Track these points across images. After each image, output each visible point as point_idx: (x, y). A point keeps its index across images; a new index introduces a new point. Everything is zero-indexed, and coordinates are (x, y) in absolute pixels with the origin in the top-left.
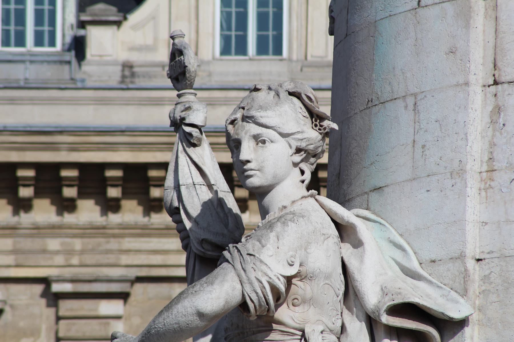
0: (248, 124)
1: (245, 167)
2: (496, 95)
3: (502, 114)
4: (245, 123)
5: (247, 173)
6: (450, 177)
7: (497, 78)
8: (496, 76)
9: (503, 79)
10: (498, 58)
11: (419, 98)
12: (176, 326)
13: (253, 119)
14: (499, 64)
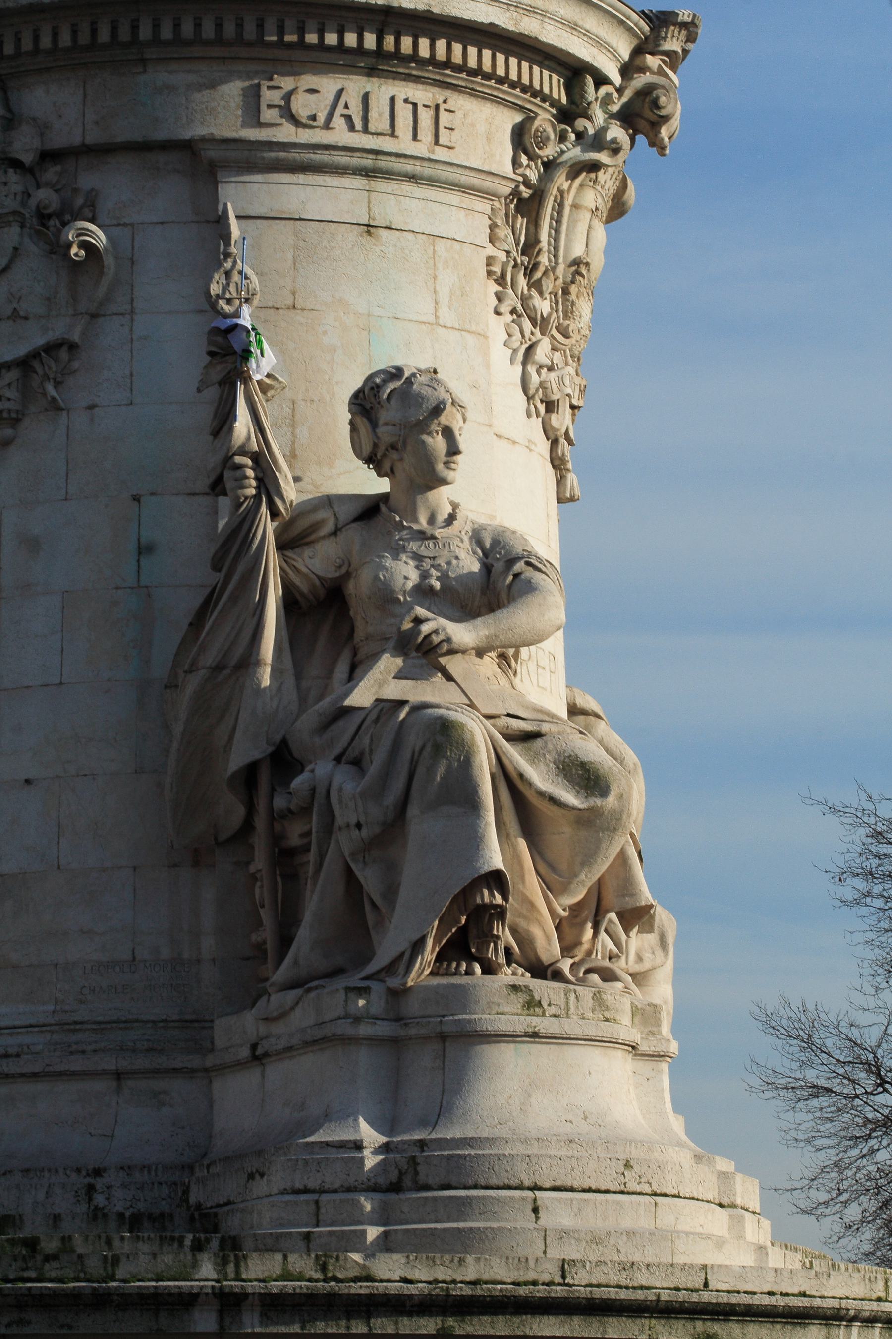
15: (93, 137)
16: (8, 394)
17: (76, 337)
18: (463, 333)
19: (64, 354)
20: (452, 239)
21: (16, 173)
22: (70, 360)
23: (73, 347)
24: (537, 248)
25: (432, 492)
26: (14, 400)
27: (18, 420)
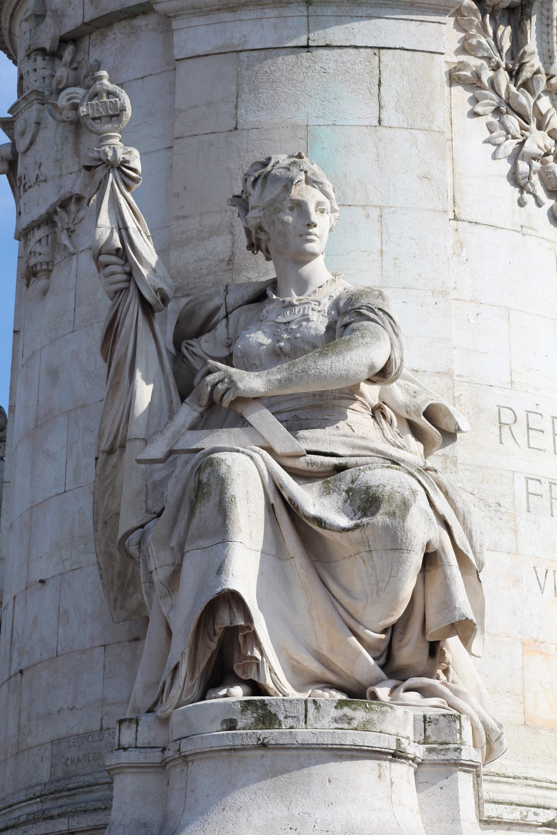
0: (313, 189)
1: (310, 230)
2: (457, 230)
3: (464, 249)
4: (309, 187)
5: (309, 237)
6: (431, 295)
7: (457, 215)
8: (456, 212)
9: (463, 217)
10: (458, 196)
11: (386, 211)
12: (343, 372)
13: (321, 186)
14: (458, 201)
15: (91, 14)
16: (38, 249)
17: (77, 190)
18: (412, 131)
19: (73, 207)
20: (400, 49)
21: (44, 59)
22: (78, 211)
23: (79, 199)
24: (522, 51)
25: (307, 265)
26: (44, 254)
27: (50, 271)
